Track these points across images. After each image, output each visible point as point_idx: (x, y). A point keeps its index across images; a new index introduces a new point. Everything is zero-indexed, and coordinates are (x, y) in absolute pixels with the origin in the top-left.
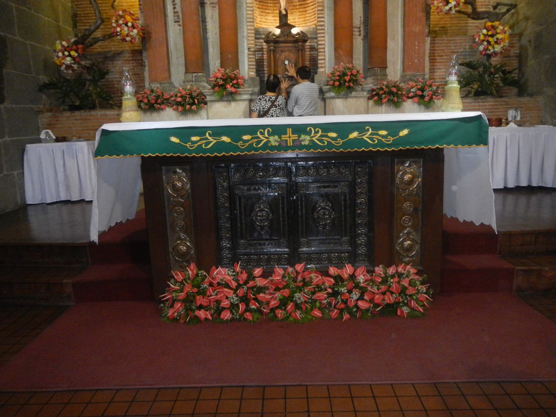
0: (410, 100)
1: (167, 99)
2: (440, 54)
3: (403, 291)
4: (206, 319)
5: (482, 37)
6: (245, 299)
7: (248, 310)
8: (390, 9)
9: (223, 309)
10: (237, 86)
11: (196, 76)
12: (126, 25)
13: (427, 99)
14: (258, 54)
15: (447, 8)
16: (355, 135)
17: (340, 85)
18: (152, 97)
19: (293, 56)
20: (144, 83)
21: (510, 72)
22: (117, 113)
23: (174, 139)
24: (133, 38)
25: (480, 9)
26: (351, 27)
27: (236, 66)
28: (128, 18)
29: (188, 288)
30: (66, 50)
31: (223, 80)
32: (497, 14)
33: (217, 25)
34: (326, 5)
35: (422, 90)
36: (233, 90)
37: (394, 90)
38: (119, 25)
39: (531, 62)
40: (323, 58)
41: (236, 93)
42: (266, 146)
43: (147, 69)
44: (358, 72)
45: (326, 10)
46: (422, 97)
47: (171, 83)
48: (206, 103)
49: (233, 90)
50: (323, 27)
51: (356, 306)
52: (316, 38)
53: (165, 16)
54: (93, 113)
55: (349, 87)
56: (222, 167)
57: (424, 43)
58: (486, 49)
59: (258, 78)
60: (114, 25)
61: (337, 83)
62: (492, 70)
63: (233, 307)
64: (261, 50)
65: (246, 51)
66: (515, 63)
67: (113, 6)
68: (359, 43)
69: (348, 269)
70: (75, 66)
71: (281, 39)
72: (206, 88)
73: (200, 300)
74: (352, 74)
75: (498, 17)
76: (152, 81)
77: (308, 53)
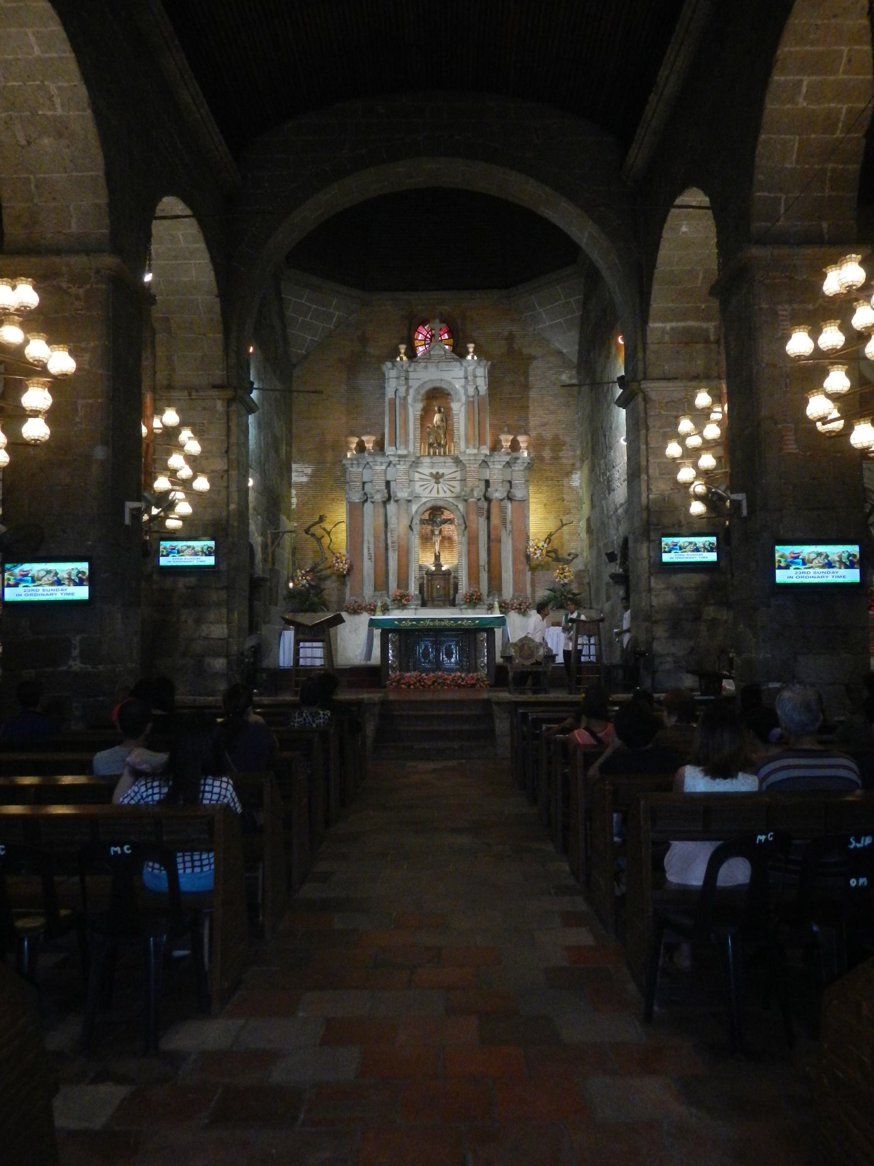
0: (513, 611)
1: (365, 607)
3: (478, 680)
4: (405, 688)
5: (557, 574)
6: (419, 681)
7: (421, 685)
8: (503, 555)
9: (412, 684)
10: (408, 600)
12: (342, 562)
13: (523, 610)
15: (536, 557)
16: (460, 622)
17: (470, 601)
18: (356, 606)
19: (442, 583)
21: (578, 594)
23: (396, 622)
24: (344, 569)
25: (560, 556)
26: (478, 566)
27: (407, 588)
28: (344, 558)
29: (398, 678)
30: (303, 576)
31: (401, 597)
32: (567, 560)
33: (397, 563)
34: (463, 553)
35: (520, 605)
36: (406, 603)
37: (503, 604)
38: (338, 562)
39: (592, 588)
41: (407, 605)
42: (428, 625)
43: (348, 587)
44: (481, 594)
45: (463, 555)
46: (520, 609)
47: (364, 597)
48: (388, 610)
49: (406, 603)
51: (460, 684)
52: (457, 571)
53: (363, 555)
54: (318, 614)
55: (475, 603)
57: (526, 573)
58: (559, 581)
59: (420, 596)
60: (334, 562)
61: (468, 600)
62: (565, 594)
63: (415, 683)
64: (422, 578)
65: (413, 579)
66: (587, 588)
67: (329, 548)
68: (484, 576)
69: (459, 674)
70: (307, 585)
71: (435, 573)
72: (389, 601)
73: (402, 681)
74: (477, 595)
75: (568, 562)
76: (352, 595)
77: (452, 581)
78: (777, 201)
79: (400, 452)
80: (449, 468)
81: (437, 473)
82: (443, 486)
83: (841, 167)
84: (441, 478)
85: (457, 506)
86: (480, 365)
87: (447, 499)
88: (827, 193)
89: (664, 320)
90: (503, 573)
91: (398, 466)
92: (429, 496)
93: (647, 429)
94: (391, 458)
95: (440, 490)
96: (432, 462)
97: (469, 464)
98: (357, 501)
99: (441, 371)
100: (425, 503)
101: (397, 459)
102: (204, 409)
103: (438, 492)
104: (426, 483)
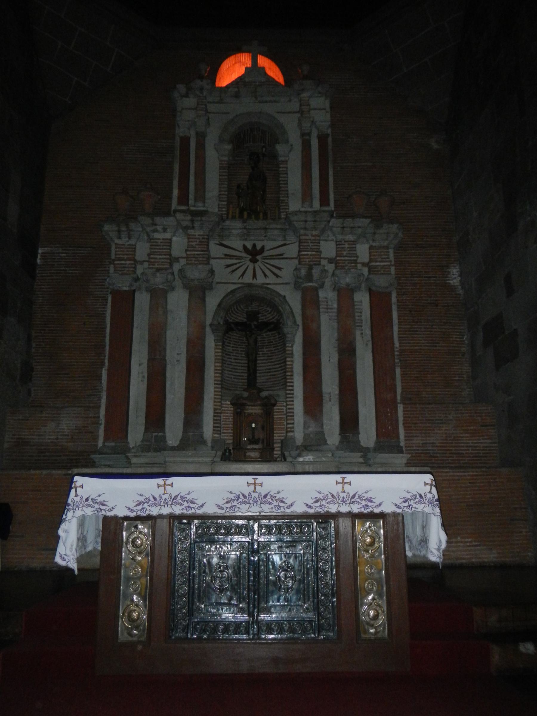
2: (415, 422)
11: (157, 436)
14: (224, 416)
20: (97, 442)
22: (64, 473)
40: (292, 422)
50: (292, 392)
56: (184, 524)
81: (254, 246)
82: (263, 267)
84: (259, 255)
85: (285, 297)
86: (320, 93)
87: (269, 286)
90: (360, 406)
91: (191, 232)
92: (240, 281)
95: (259, 273)
96: (245, 228)
97: (305, 229)
98: (125, 288)
99: (260, 102)
100: (233, 292)
101: (189, 218)
103: (254, 276)
104: (234, 261)
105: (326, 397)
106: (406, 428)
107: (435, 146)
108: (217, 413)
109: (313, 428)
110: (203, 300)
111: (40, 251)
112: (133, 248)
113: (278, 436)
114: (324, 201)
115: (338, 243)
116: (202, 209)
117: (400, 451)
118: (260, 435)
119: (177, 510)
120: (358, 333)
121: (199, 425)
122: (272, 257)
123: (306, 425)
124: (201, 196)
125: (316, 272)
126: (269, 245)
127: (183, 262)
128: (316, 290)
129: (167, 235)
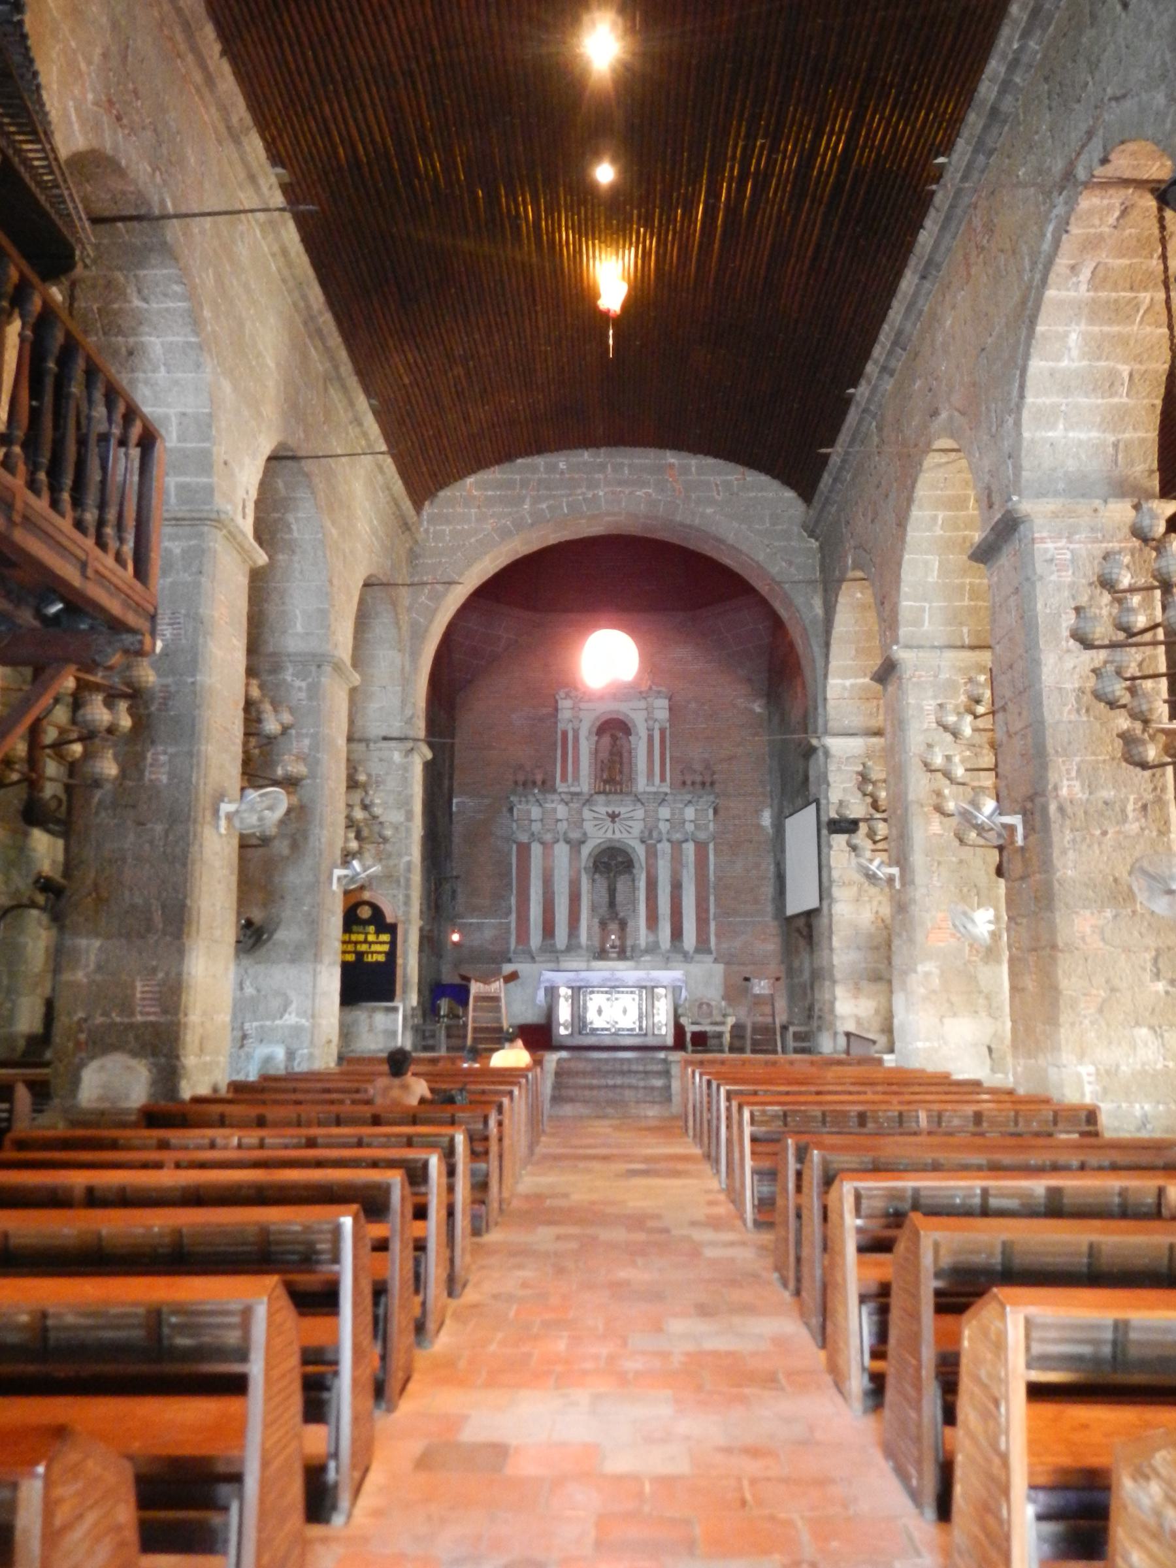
78: (923, 609)
79: (573, 789)
80: (626, 806)
83: (978, 581)
88: (966, 603)
89: (844, 677)
93: (828, 785)
94: (563, 796)
102: (381, 760)
105: (661, 917)
106: (717, 936)
107: (758, 710)
108: (589, 928)
109: (651, 939)
110: (579, 852)
111: (455, 801)
112: (529, 812)
113: (629, 943)
114: (663, 779)
115: (672, 810)
116: (577, 789)
117: (709, 952)
118: (618, 943)
119: (582, 984)
120: (685, 872)
121: (578, 937)
122: (626, 819)
123: (647, 936)
124: (576, 777)
125: (655, 834)
126: (623, 810)
127: (565, 824)
128: (655, 846)
129: (553, 805)
